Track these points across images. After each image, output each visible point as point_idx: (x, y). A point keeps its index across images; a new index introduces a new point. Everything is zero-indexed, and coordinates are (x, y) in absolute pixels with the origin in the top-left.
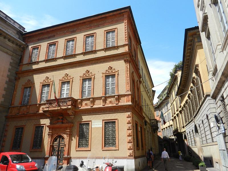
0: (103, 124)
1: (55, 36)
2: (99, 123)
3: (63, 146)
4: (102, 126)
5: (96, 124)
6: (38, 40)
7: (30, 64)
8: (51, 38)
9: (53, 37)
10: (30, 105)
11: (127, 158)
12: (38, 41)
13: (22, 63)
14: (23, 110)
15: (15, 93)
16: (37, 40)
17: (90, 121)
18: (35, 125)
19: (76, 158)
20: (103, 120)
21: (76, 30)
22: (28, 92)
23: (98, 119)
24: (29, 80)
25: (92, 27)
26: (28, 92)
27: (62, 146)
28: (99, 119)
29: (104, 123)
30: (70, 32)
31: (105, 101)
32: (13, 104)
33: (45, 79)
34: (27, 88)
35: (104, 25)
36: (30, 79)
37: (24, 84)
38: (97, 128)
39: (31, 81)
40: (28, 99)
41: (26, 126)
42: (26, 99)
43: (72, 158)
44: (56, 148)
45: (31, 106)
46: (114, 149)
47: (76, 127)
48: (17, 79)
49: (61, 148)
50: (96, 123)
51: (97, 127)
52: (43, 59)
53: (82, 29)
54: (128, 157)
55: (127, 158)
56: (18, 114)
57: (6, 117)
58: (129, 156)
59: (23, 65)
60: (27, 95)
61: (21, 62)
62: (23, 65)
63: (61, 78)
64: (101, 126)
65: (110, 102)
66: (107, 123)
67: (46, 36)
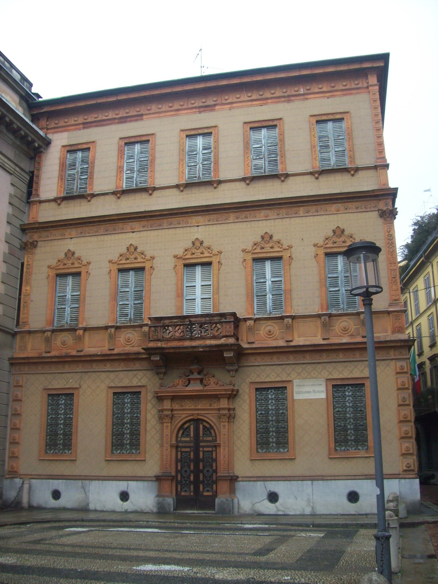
0: (327, 390)
1: (142, 115)
2: (317, 388)
3: (210, 449)
4: (327, 395)
5: (310, 391)
6: (84, 124)
7: (64, 202)
8: (130, 121)
9: (136, 120)
10: (85, 329)
11: (400, 476)
12: (84, 128)
13: (38, 195)
14: (64, 343)
15: (28, 288)
16: (81, 126)
17: (290, 381)
18: (110, 387)
19: (255, 479)
20: (327, 380)
21: (215, 105)
22: (69, 288)
23: (313, 378)
24: (69, 250)
25: (267, 99)
26: (69, 288)
27: (206, 449)
28: (316, 378)
29: (330, 388)
30: (196, 108)
31: (326, 327)
32: (26, 323)
33: (124, 250)
34: (66, 275)
35: (307, 99)
36: (72, 249)
37: (53, 263)
38: (310, 402)
39: (76, 255)
40: (76, 311)
41: (81, 391)
42: (68, 310)
43: (240, 479)
44: (189, 452)
45: (87, 334)
46: (363, 456)
47: (246, 397)
48: (28, 247)
49: (204, 452)
50: (306, 389)
51: (311, 399)
52: (111, 187)
53: (235, 102)
54: (401, 473)
55: (400, 476)
56: (49, 355)
57: (10, 362)
58: (405, 471)
59: (41, 202)
60: (69, 296)
61: (34, 192)
62: (41, 202)
63: (180, 252)
64: (323, 396)
65: (345, 330)
66: (337, 387)
67: (111, 114)
